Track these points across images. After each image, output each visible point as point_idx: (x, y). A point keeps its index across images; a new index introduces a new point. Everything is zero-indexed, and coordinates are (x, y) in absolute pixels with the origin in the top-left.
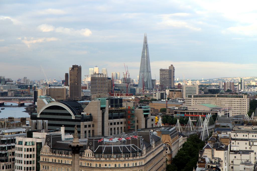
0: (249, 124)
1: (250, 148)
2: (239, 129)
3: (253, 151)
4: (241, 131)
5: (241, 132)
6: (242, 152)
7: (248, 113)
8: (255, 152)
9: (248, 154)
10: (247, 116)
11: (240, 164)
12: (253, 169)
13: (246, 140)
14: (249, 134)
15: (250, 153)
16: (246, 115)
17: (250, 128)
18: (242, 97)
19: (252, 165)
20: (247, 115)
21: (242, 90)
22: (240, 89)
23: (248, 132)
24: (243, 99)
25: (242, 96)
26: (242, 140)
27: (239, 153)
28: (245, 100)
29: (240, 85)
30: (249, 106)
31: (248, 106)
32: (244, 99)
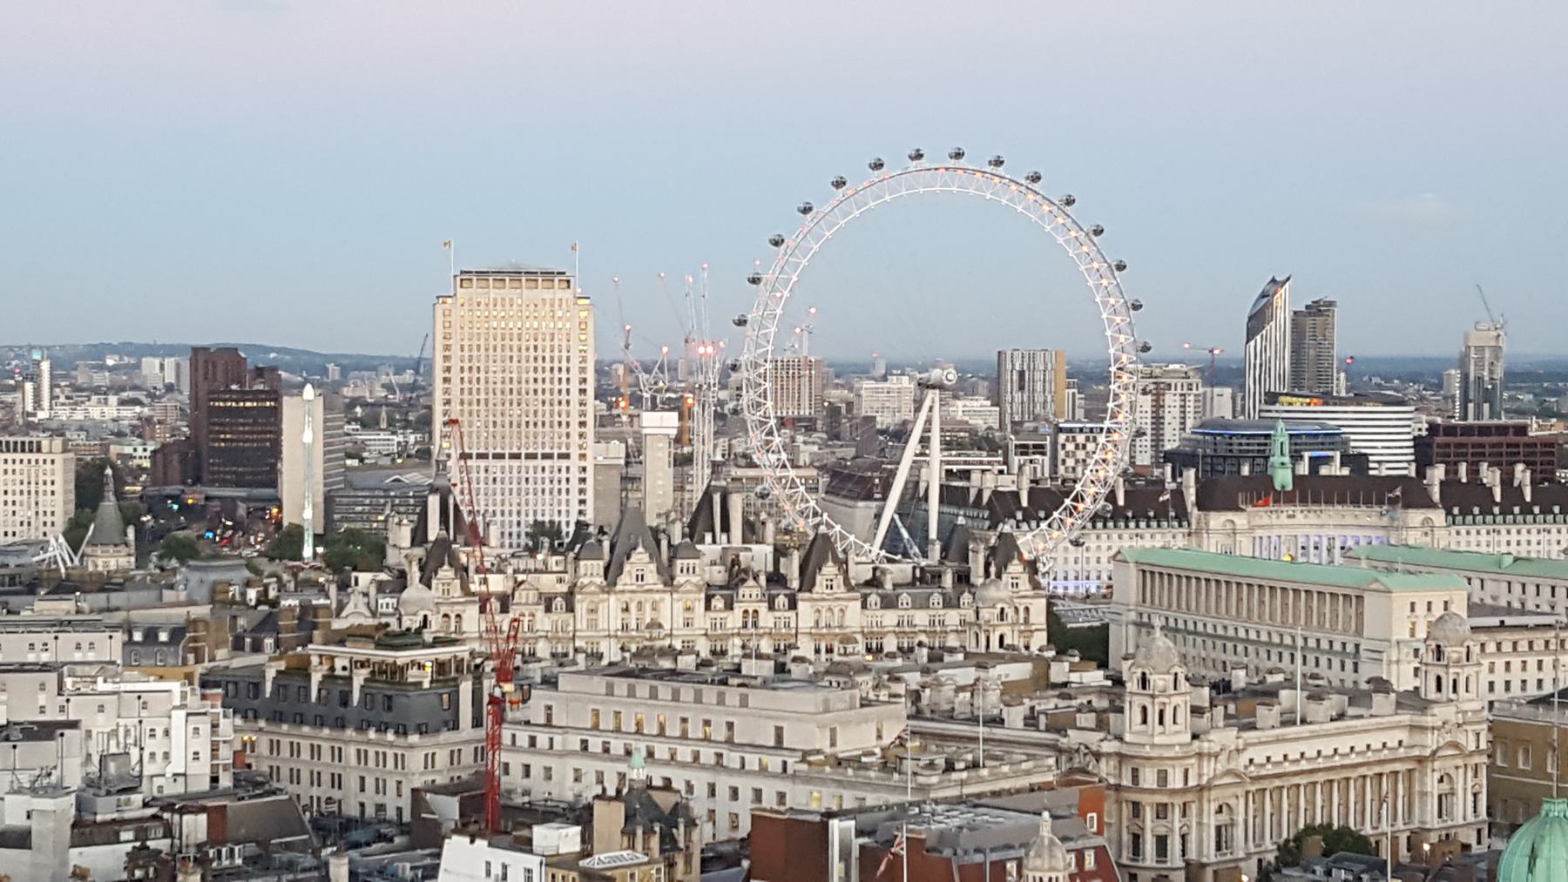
0: (63, 587)
1: (62, 709)
2: (9, 612)
3: (74, 725)
4: (17, 624)
5: (21, 630)
6: (22, 730)
7: (65, 534)
8: (84, 726)
9: (50, 737)
10: (58, 548)
11: (8, 793)
12: (73, 811)
13: (40, 671)
14: (60, 635)
15: (62, 735)
16: (53, 541)
17: (62, 607)
18: (39, 450)
19: (68, 794)
20: (62, 539)
21: (42, 415)
22: (30, 408)
23: (62, 625)
24: (41, 457)
25: (39, 443)
26: (23, 668)
27: (7, 739)
28: (53, 462)
29: (29, 386)
30: (72, 496)
31: (66, 492)
32: (49, 457)
